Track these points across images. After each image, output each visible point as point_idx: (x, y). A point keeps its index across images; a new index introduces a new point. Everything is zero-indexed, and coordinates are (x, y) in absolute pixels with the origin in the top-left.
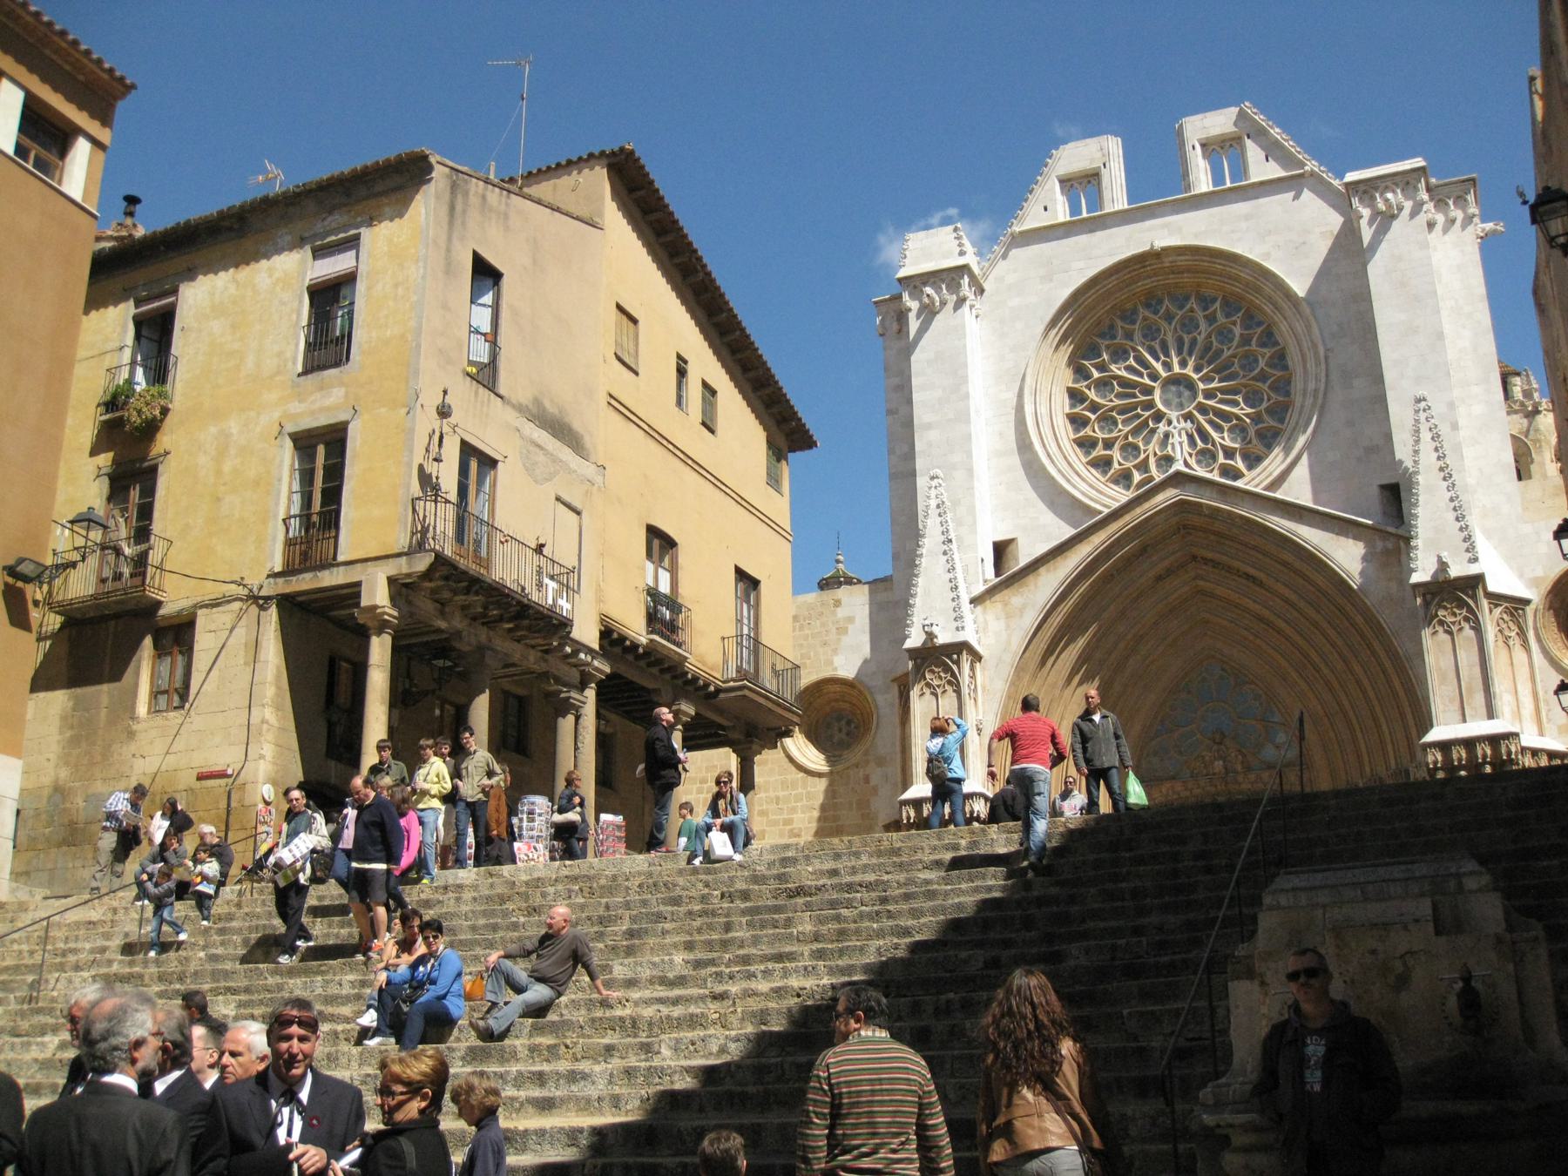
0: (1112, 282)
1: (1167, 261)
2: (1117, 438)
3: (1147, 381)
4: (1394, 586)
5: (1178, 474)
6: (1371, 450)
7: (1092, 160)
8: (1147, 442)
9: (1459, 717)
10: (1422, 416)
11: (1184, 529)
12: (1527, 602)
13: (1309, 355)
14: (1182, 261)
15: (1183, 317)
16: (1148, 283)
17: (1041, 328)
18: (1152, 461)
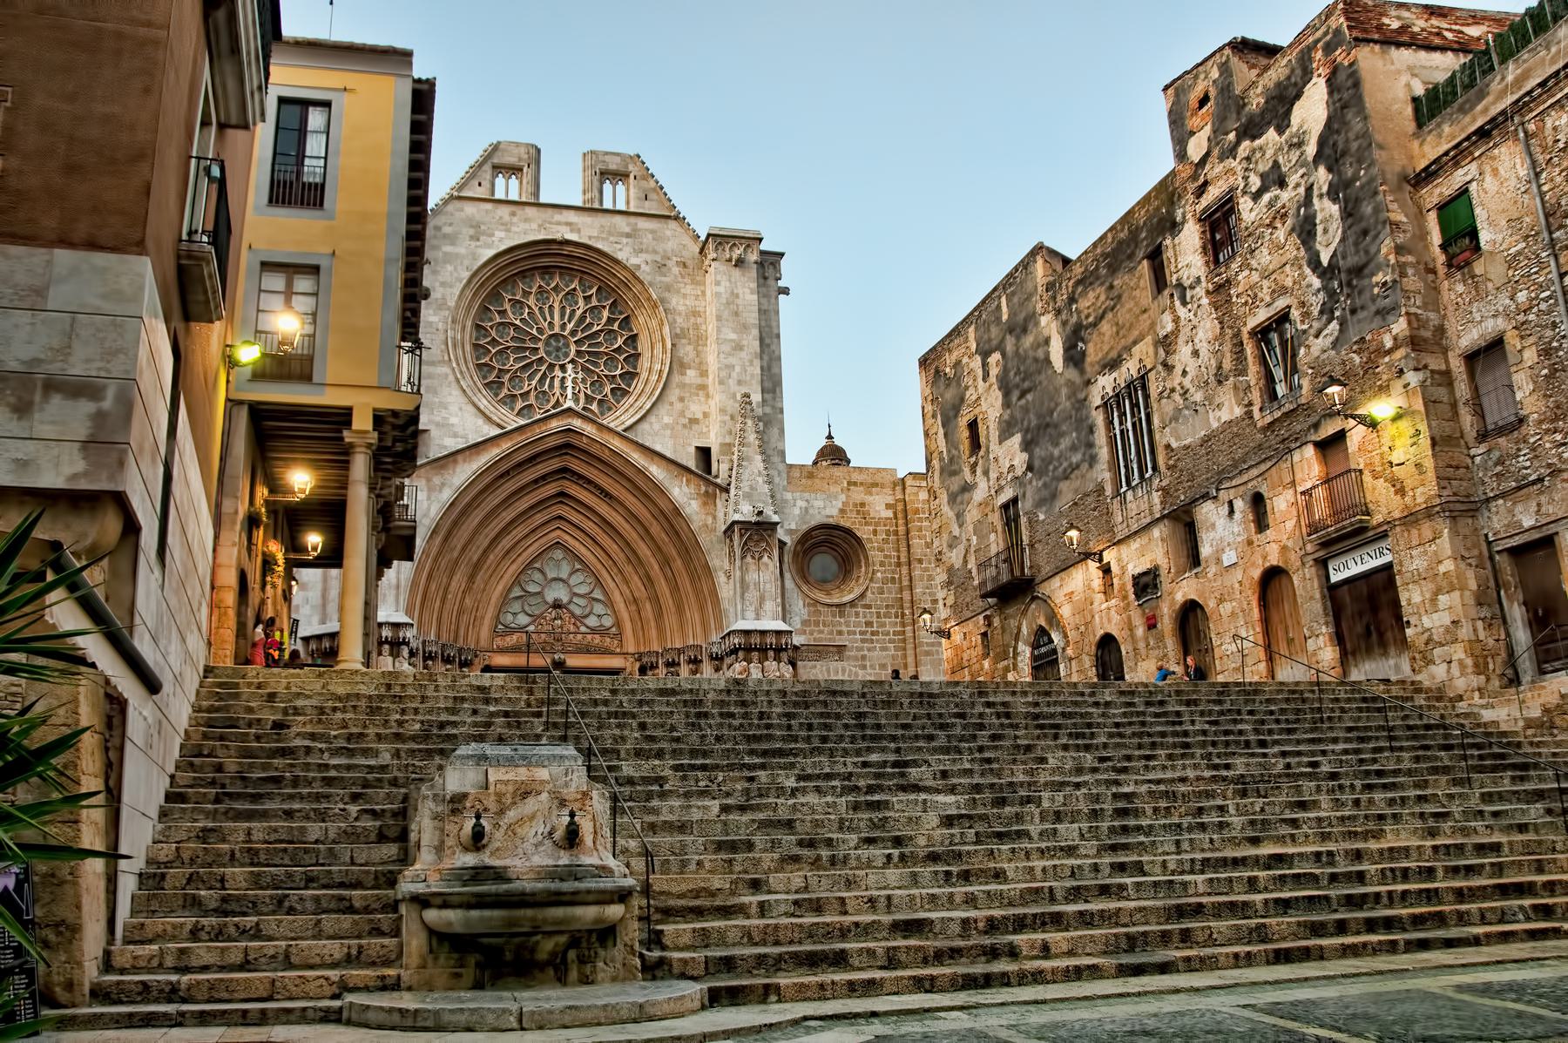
0: (524, 253)
1: (568, 249)
2: (509, 371)
3: (534, 332)
4: (710, 520)
5: (569, 409)
6: (693, 421)
7: (520, 160)
8: (530, 378)
9: (753, 615)
10: (748, 407)
11: (566, 448)
12: (785, 544)
13: (659, 347)
14: (579, 252)
15: (568, 293)
16: (545, 261)
17: (466, 275)
18: (533, 394)
